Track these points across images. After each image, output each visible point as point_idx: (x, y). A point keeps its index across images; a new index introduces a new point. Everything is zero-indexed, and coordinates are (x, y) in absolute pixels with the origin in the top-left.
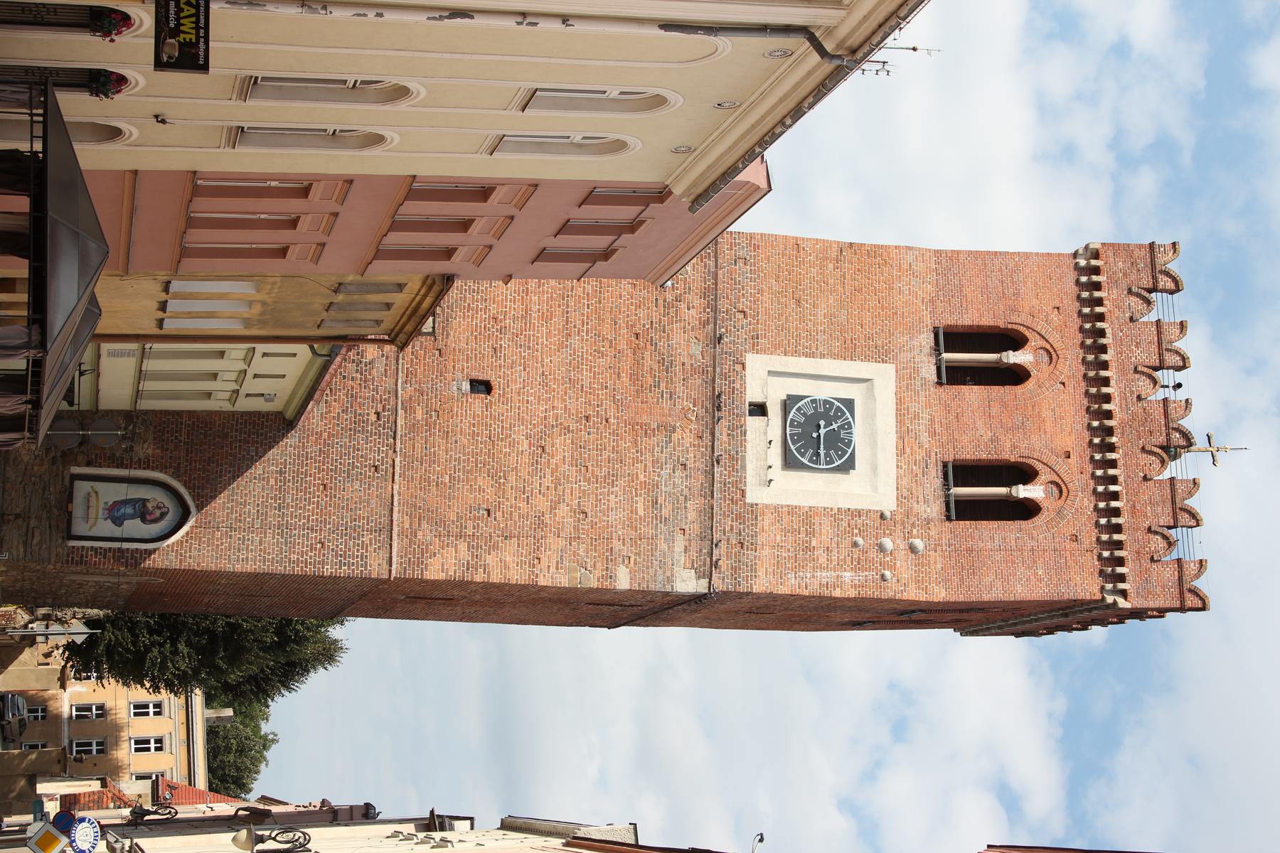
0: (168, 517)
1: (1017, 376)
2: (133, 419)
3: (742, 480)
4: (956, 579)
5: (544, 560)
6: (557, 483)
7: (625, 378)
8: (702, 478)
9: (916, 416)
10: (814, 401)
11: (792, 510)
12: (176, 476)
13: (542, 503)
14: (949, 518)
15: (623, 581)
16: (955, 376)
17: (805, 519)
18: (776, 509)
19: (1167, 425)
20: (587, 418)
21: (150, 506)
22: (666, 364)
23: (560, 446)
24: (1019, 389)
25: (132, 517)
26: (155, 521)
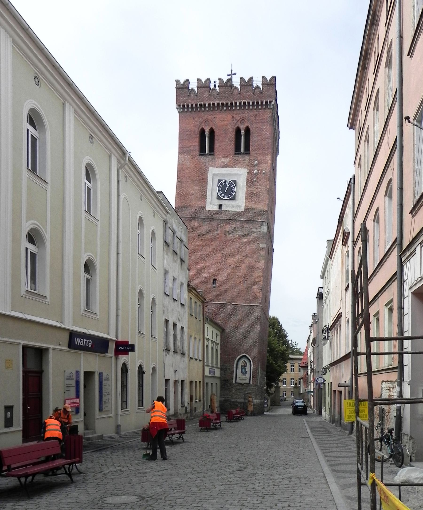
0: (245, 360)
1: (212, 132)
2: (222, 369)
3: (238, 212)
4: (266, 152)
5: (258, 266)
6: (238, 262)
7: (212, 243)
8: (238, 223)
9: (222, 162)
10: (218, 191)
11: (247, 198)
12: (236, 359)
13: (243, 267)
14: (249, 153)
15: (263, 245)
16: (212, 149)
17: (249, 195)
18: (246, 203)
19: (226, 86)
20: (223, 253)
21: (243, 365)
22: (209, 232)
23: (230, 261)
24: (215, 131)
25: (245, 369)
26: (246, 363)
